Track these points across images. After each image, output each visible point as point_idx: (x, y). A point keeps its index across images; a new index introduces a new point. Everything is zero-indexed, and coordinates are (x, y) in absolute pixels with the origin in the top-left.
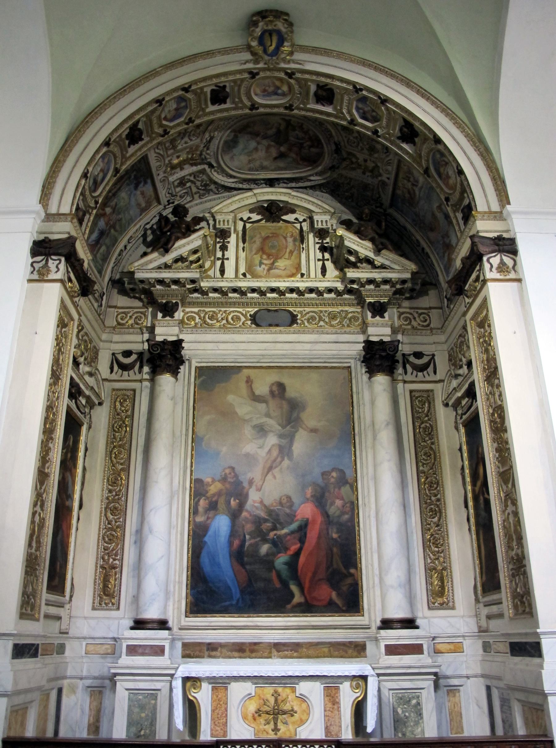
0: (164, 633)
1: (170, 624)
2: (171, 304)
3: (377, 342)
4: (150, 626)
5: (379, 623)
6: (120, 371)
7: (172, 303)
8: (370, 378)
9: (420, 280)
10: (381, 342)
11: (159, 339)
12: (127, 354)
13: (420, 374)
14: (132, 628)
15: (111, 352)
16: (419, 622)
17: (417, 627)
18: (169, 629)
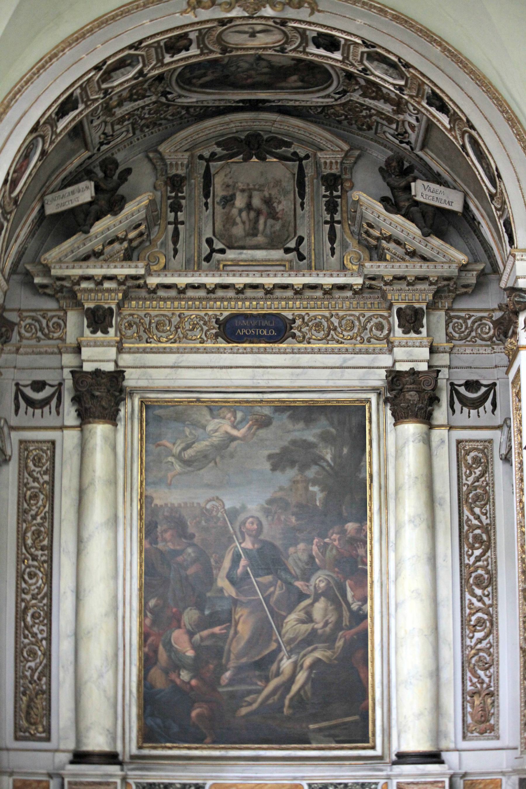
0: (114, 769)
1: (120, 758)
2: (101, 312)
3: (406, 372)
4: (96, 759)
5: (394, 758)
6: (30, 410)
7: (104, 307)
8: (395, 425)
9: (475, 273)
10: (413, 372)
11: (88, 367)
12: (38, 386)
13: (473, 412)
14: (72, 762)
15: (14, 383)
16: (445, 756)
17: (442, 762)
18: (120, 763)
